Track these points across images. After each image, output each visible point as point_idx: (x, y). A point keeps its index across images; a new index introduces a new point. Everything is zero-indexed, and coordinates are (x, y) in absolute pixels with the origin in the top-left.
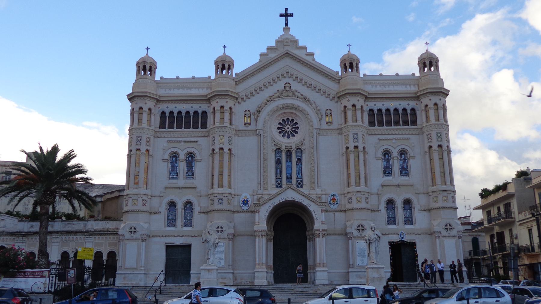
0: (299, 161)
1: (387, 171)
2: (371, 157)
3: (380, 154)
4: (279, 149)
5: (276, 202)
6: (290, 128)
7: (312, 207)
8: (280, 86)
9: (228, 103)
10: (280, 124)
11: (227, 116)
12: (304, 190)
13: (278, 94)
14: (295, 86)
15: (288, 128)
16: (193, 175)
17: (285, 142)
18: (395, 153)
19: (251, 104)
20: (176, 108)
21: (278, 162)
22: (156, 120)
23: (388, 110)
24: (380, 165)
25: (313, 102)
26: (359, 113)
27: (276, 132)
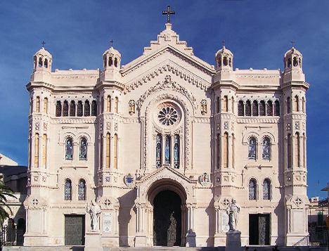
0: (177, 145)
1: (253, 155)
2: (238, 143)
3: (246, 140)
4: (160, 135)
5: (154, 179)
6: (170, 116)
7: (185, 184)
8: (161, 78)
9: (117, 93)
10: (161, 112)
11: (113, 103)
12: (181, 170)
13: (158, 86)
14: (175, 78)
15: (168, 116)
16: (85, 156)
17: (165, 129)
18: (260, 140)
19: (135, 95)
20: (69, 97)
21: (159, 146)
22: (53, 109)
23: (255, 102)
24: (247, 149)
25: (190, 94)
26: (230, 102)
27: (157, 120)
